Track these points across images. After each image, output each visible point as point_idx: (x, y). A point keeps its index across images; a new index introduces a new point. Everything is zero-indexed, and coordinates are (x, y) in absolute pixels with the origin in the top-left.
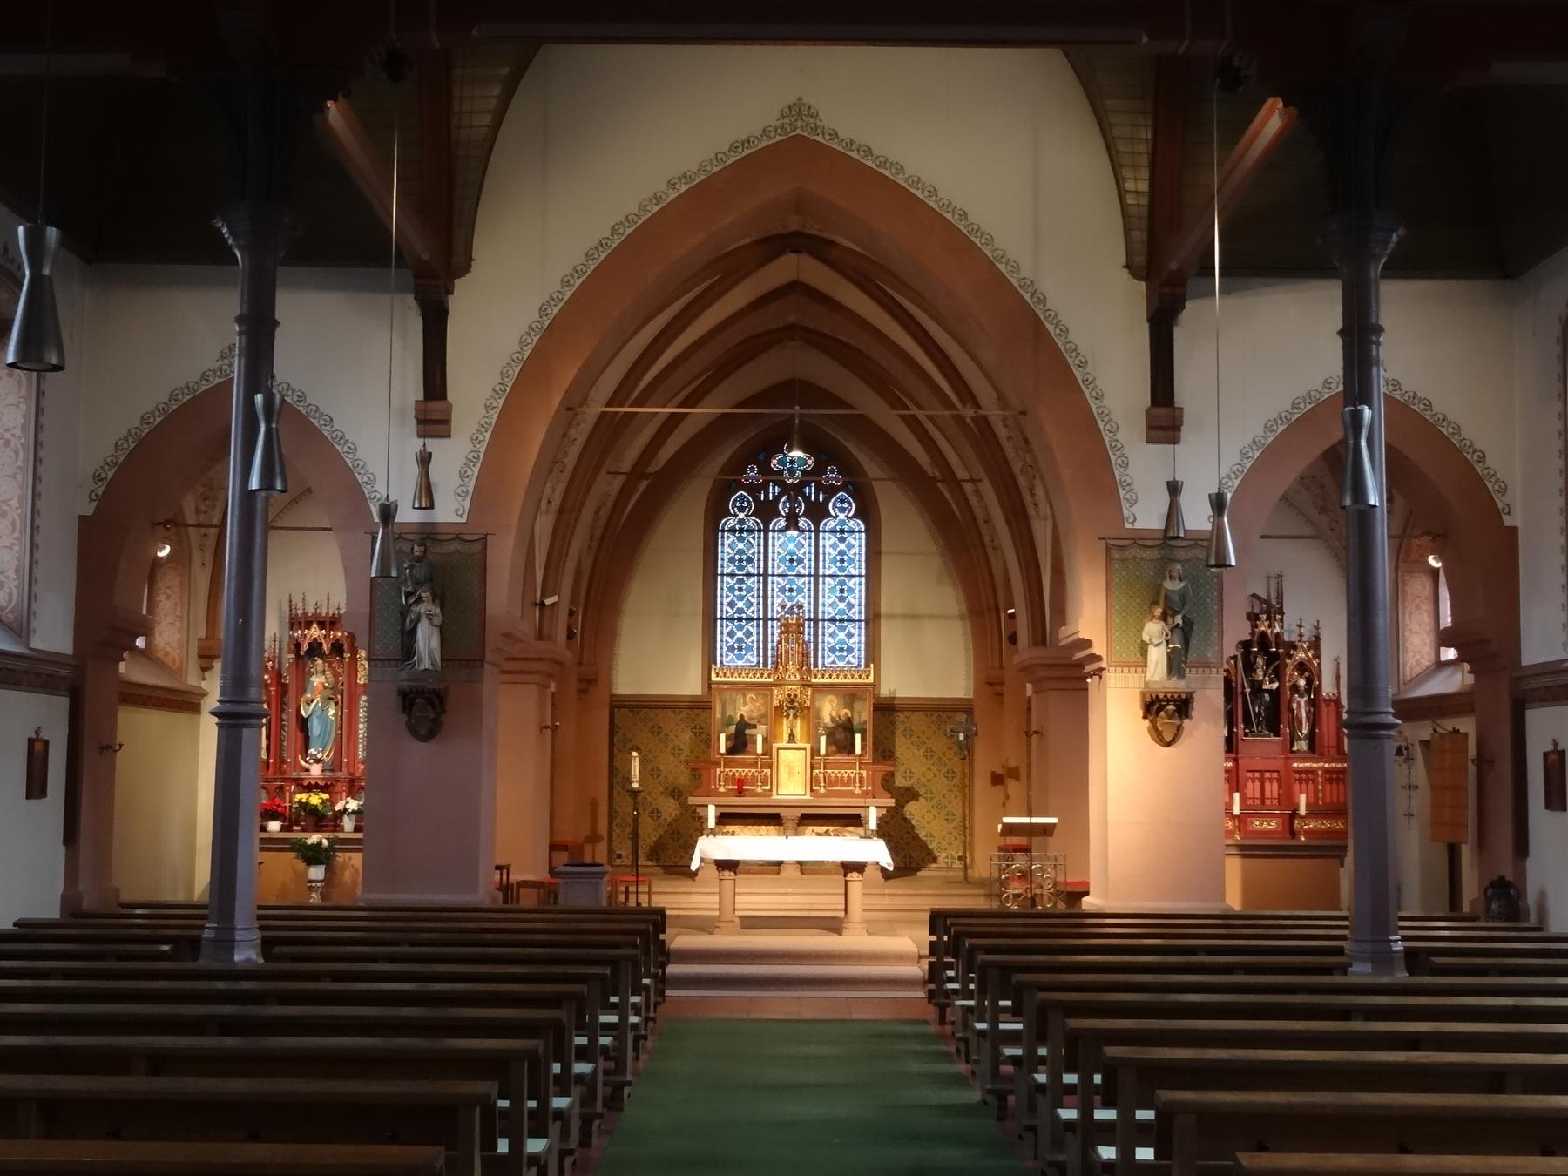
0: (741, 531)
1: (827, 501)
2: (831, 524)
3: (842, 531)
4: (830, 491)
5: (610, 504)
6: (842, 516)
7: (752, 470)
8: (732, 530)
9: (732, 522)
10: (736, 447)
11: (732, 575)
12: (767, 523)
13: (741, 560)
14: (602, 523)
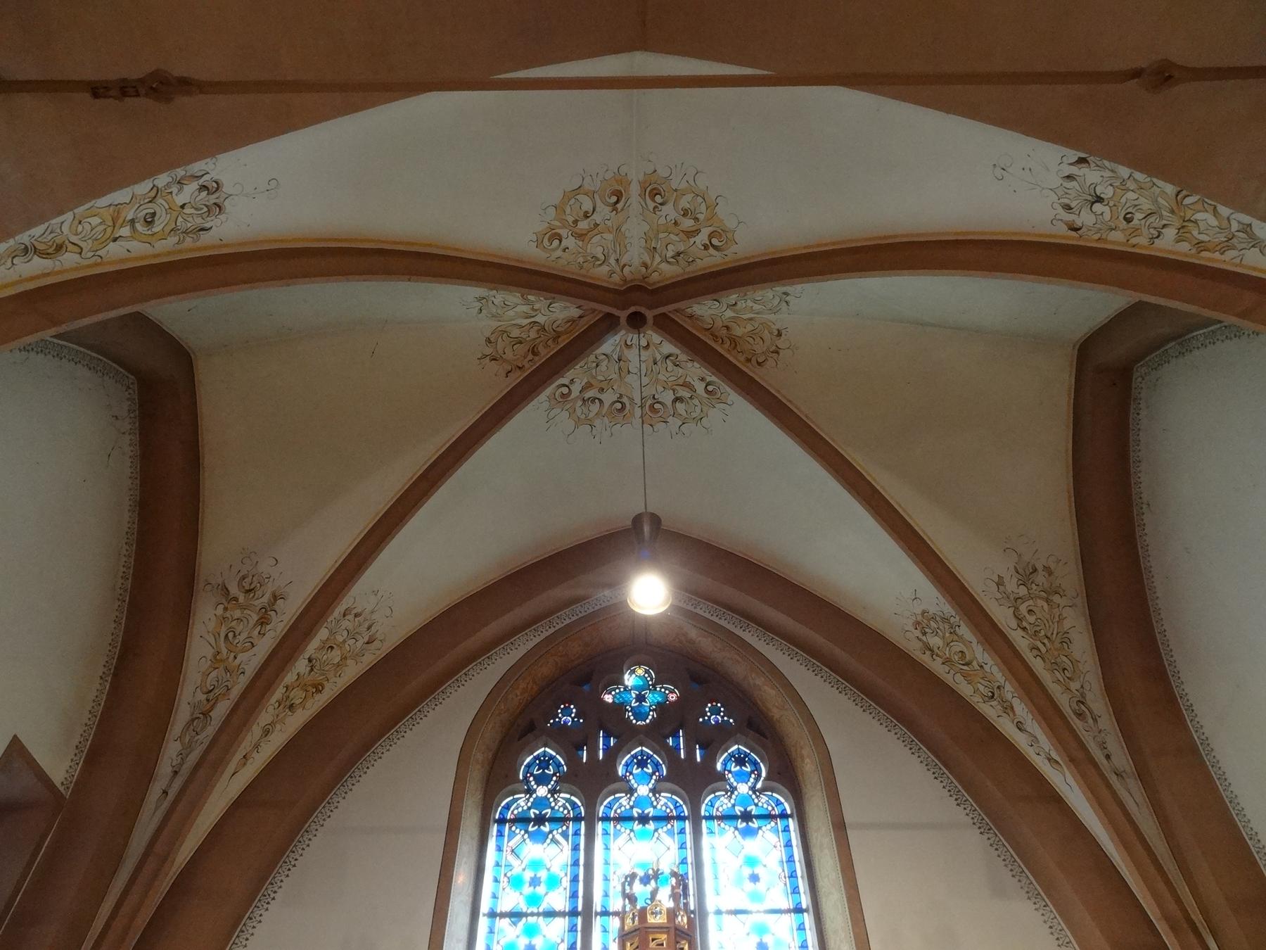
0: (540, 820)
1: (710, 759)
2: (723, 804)
3: (747, 817)
4: (712, 741)
5: (236, 692)
6: (743, 789)
7: (567, 712)
8: (522, 820)
9: (521, 803)
10: (531, 645)
11: (516, 915)
12: (591, 805)
13: (535, 882)
14: (211, 731)
